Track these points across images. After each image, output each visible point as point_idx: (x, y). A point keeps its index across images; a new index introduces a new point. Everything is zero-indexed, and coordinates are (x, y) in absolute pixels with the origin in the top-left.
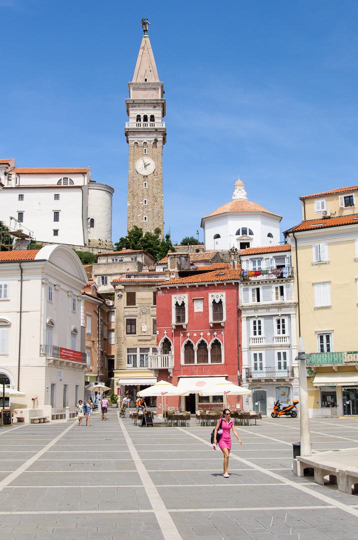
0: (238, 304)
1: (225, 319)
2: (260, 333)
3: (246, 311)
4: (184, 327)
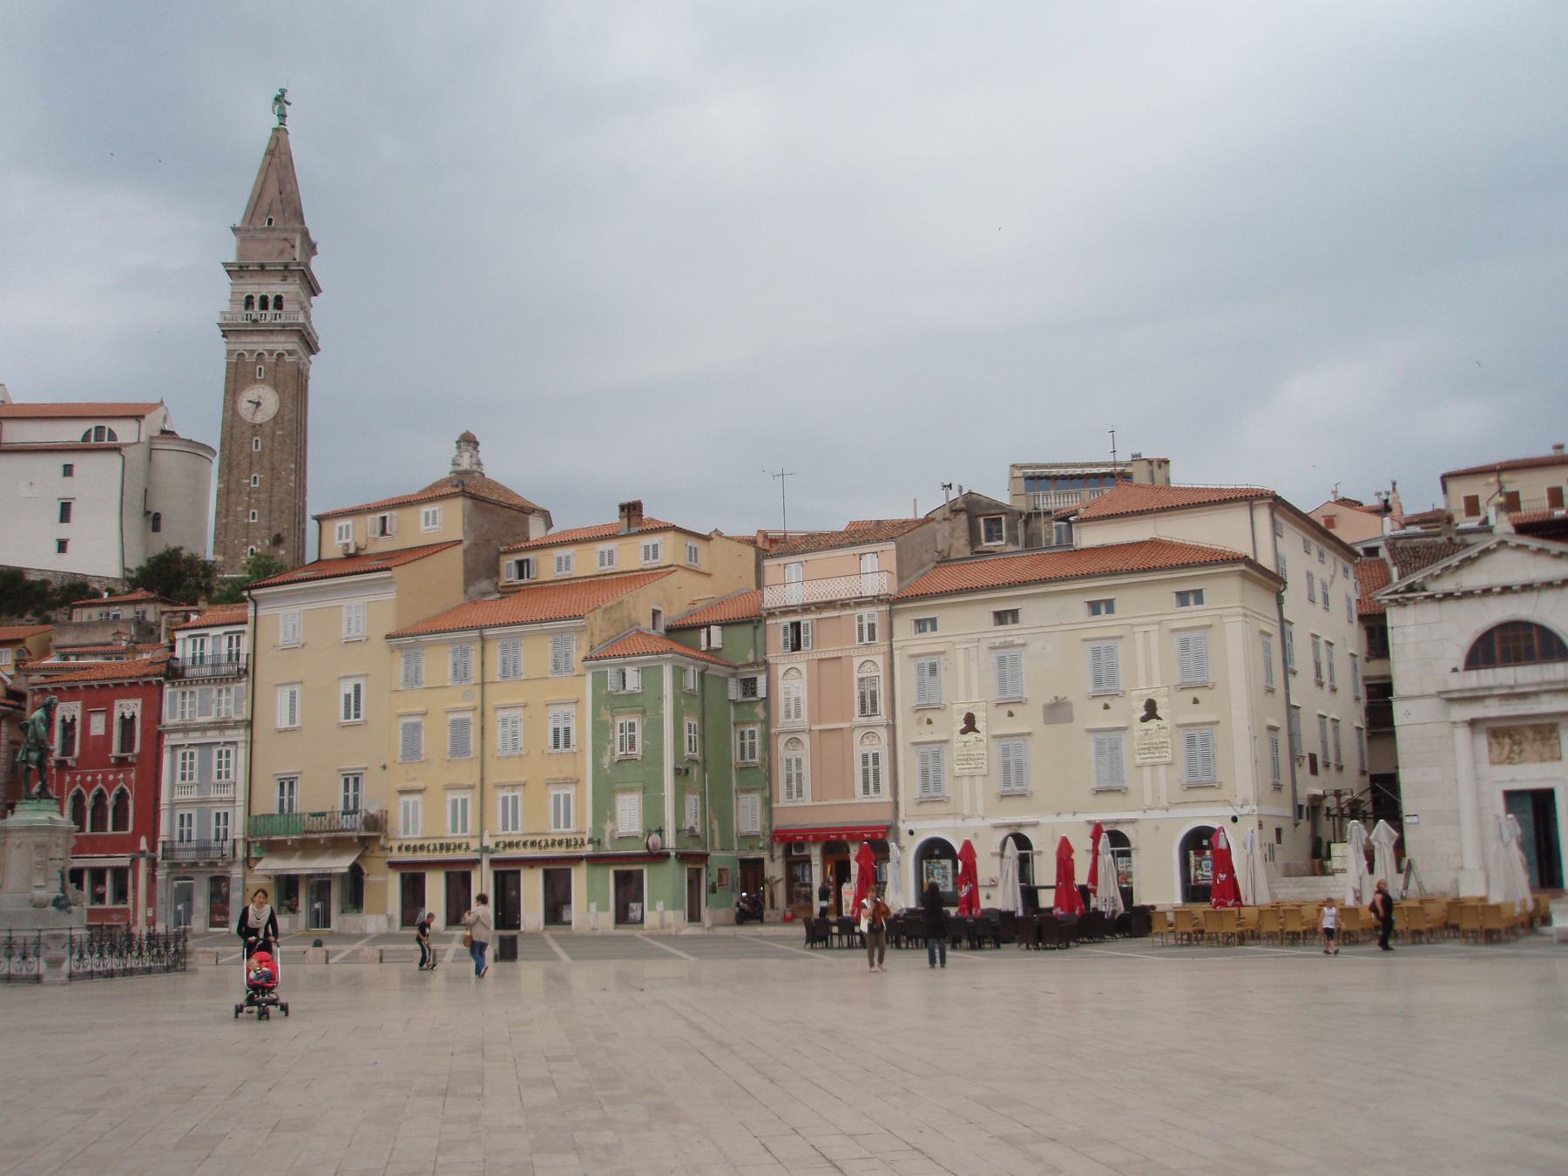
0: (159, 721)
1: (137, 749)
2: (191, 778)
3: (173, 736)
4: (70, 762)
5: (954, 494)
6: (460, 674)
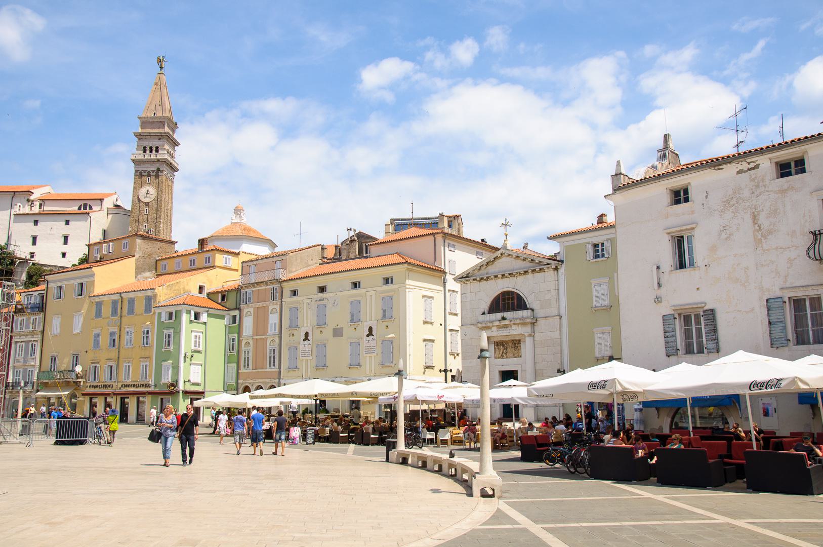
5: (352, 233)
6: (114, 312)
